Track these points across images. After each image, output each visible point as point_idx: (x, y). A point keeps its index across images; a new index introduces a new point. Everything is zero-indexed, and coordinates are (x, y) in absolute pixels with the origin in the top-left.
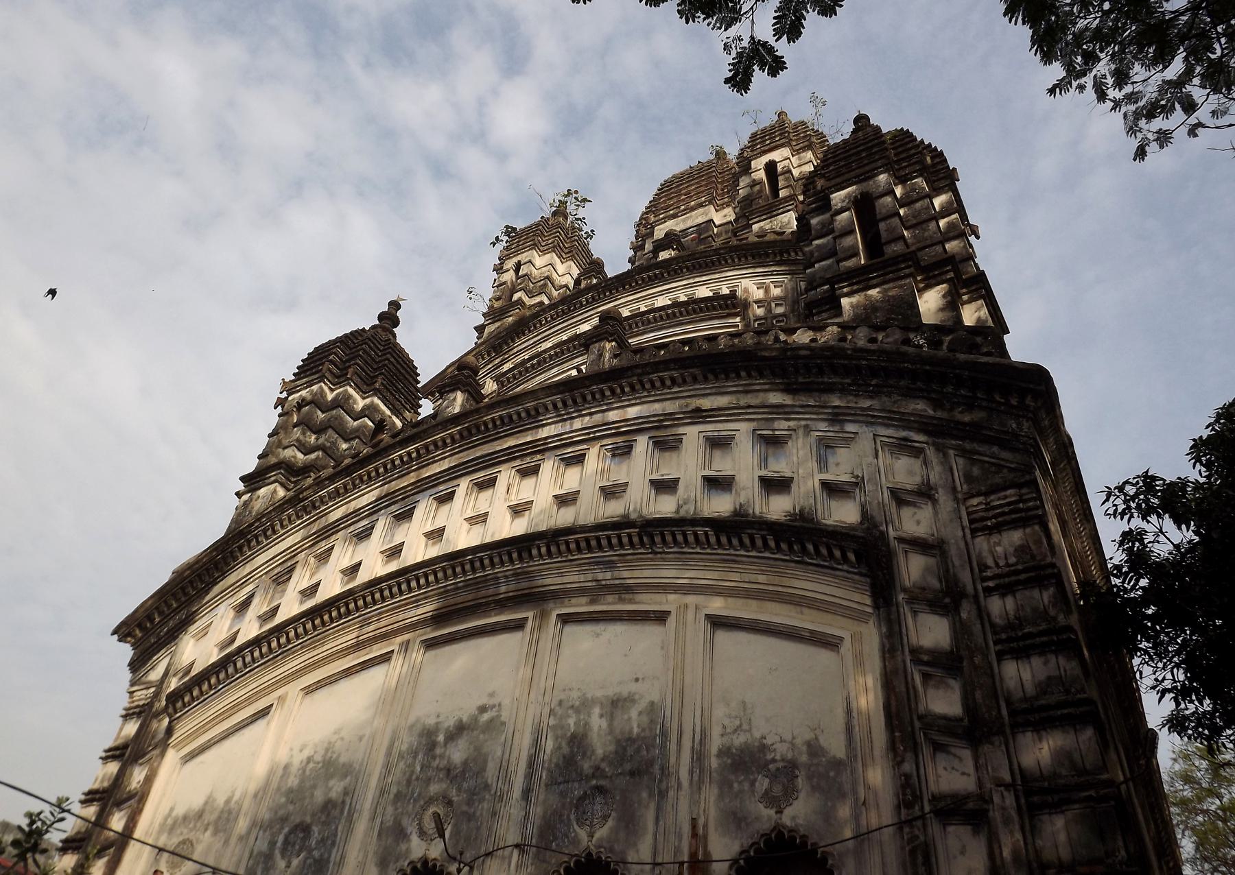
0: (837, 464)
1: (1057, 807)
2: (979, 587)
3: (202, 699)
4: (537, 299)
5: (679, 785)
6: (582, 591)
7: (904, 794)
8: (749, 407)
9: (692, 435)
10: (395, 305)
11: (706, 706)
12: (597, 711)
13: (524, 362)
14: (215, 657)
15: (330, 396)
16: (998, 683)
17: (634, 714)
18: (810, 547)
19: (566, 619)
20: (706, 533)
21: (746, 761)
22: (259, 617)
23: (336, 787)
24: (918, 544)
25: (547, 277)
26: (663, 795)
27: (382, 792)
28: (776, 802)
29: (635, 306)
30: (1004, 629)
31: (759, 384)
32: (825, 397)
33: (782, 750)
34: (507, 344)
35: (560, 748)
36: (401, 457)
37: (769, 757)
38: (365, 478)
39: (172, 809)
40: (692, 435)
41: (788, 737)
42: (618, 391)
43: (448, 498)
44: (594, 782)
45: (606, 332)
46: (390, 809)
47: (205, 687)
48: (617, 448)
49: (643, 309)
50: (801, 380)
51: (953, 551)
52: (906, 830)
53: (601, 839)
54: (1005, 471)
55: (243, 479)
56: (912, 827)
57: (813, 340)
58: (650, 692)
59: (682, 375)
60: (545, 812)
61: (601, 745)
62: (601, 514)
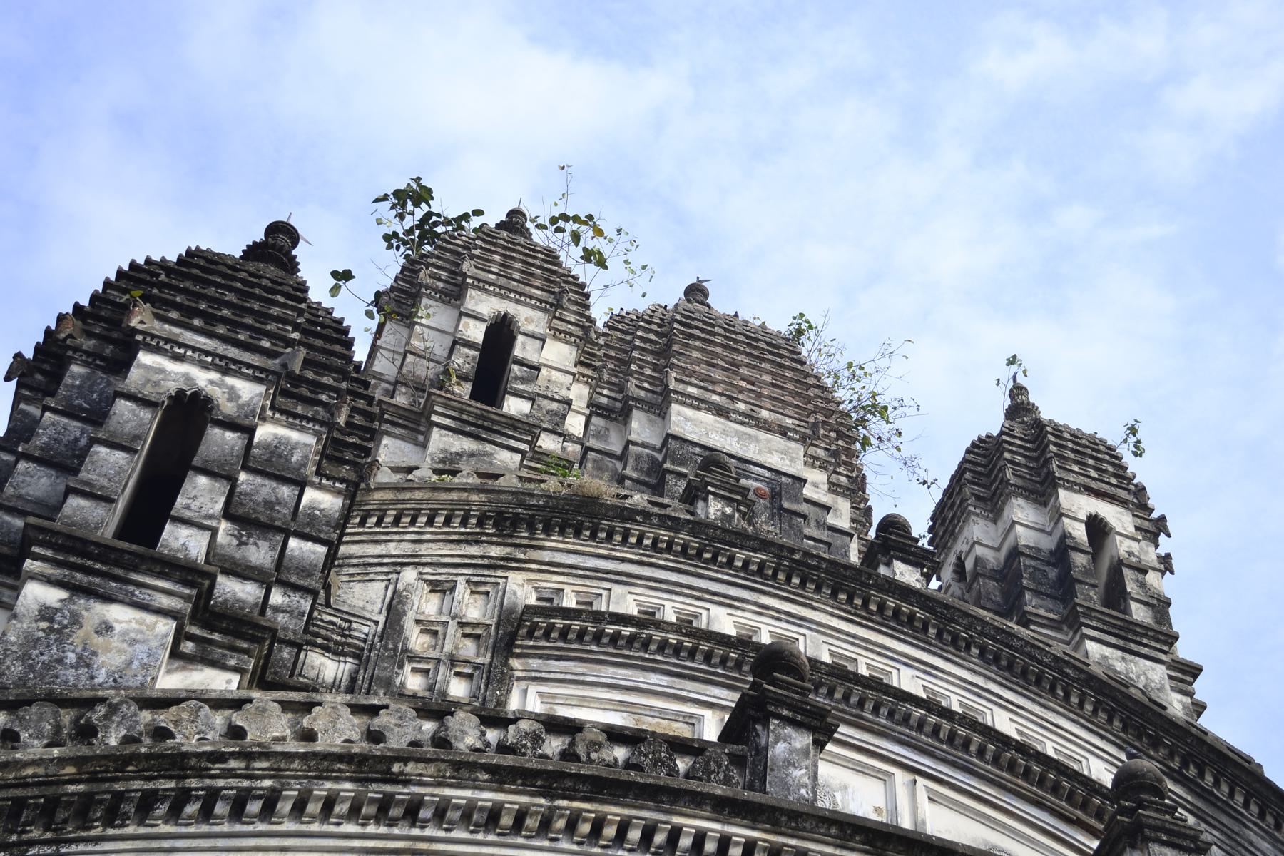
29: (847, 650)
38: (585, 828)
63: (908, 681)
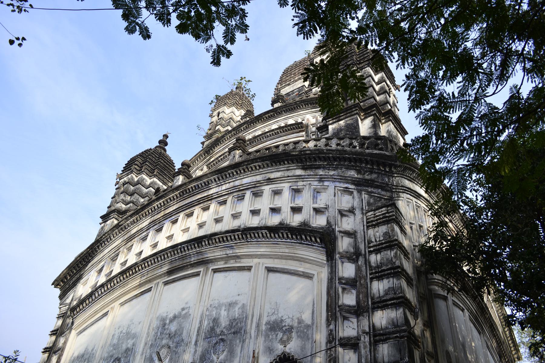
0: (321, 200)
1: (384, 341)
2: (367, 251)
3: (84, 309)
4: (226, 128)
5: (251, 337)
6: (221, 259)
7: (329, 338)
8: (288, 176)
9: (267, 189)
10: (166, 136)
11: (262, 305)
12: (224, 308)
13: (217, 158)
14: (90, 291)
15: (136, 179)
16: (369, 291)
17: (237, 309)
18: (304, 237)
19: (215, 271)
20: (266, 233)
21: (275, 326)
22: (106, 275)
23: (130, 343)
24: (348, 234)
25: (231, 118)
26: (244, 341)
27: (146, 344)
28: (284, 343)
29: (263, 130)
30: (375, 268)
31: (292, 166)
32: (317, 171)
33: (288, 322)
34: (212, 150)
35: (209, 324)
36: (157, 206)
37: (283, 325)
38: (144, 215)
39: (73, 354)
40: (267, 189)
41: (291, 316)
42: (239, 172)
43: (175, 222)
44: (220, 337)
45: (237, 146)
46: (148, 351)
47: (84, 305)
48: (239, 197)
49: (267, 130)
50: (308, 164)
51: (359, 236)
52: (329, 352)
53: (221, 360)
54: (383, 200)
55: (101, 217)
56: (331, 351)
57: (316, 146)
58: (243, 300)
59: (263, 164)
60: (202, 350)
61: (224, 322)
62: (231, 226)
63: (274, 127)
